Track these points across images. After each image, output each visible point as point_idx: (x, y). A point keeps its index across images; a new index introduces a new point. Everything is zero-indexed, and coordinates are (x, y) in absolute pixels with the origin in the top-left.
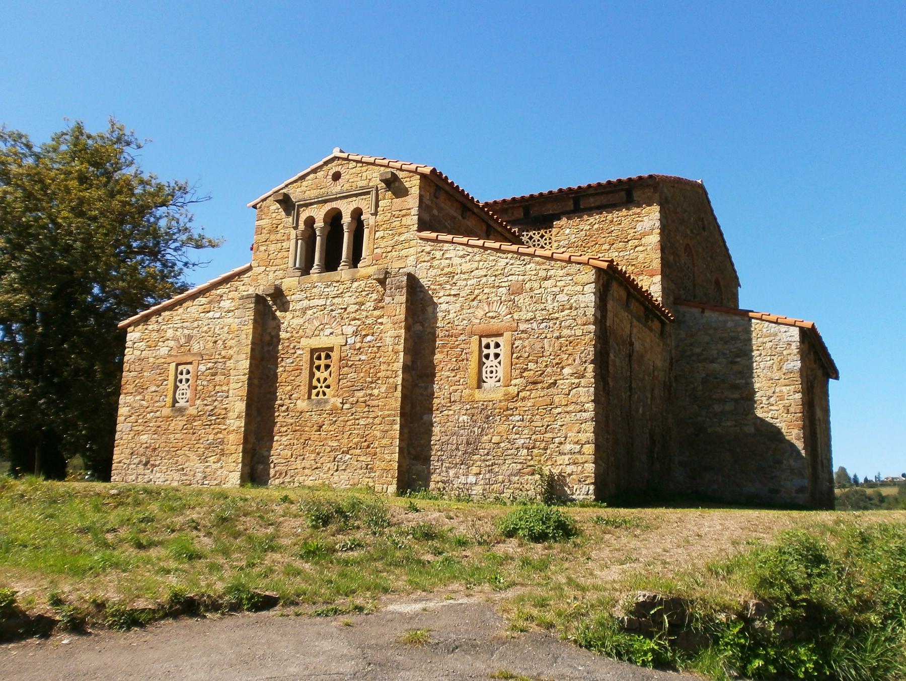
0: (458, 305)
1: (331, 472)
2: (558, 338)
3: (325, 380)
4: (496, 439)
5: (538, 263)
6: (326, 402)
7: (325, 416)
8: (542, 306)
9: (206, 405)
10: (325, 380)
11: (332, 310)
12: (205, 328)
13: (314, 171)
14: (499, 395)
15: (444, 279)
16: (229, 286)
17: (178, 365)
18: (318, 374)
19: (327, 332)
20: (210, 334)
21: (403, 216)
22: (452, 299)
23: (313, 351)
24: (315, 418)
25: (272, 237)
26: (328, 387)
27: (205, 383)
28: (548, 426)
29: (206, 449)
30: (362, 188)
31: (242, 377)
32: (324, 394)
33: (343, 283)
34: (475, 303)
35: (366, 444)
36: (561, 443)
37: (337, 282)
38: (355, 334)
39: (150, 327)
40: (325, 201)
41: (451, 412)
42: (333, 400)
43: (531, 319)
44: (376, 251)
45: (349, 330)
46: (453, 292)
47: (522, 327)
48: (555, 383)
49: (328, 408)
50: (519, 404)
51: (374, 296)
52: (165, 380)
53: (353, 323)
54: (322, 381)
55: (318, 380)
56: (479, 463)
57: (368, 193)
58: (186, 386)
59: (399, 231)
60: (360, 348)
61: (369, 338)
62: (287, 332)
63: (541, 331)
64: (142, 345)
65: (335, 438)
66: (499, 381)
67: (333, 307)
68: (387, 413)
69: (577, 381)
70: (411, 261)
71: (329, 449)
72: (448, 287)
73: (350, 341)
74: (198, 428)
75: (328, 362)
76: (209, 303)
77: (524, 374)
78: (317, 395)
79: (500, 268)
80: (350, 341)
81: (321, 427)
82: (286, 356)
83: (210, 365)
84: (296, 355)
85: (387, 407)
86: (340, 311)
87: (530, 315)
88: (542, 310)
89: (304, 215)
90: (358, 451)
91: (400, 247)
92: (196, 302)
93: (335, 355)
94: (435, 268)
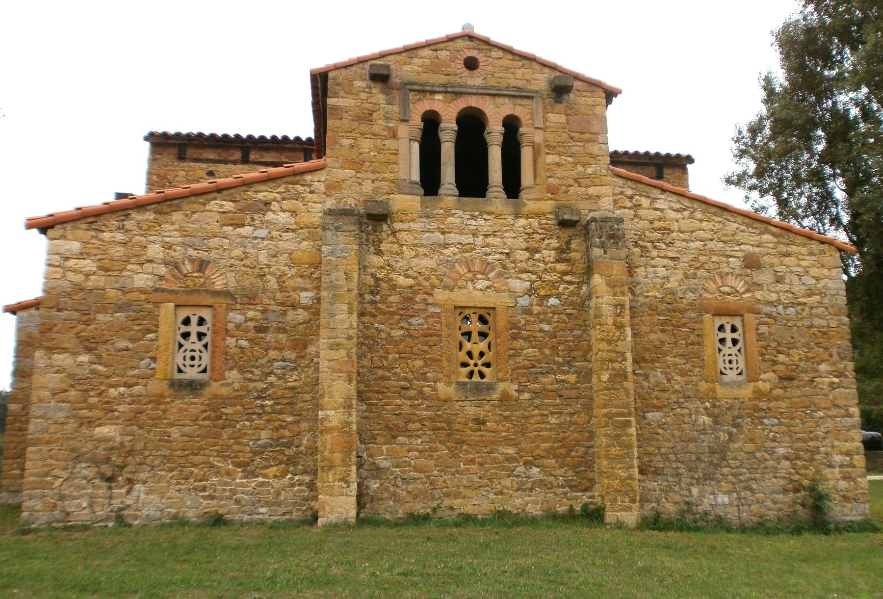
0: (681, 272)
2: (810, 327)
3: (482, 354)
4: (750, 447)
5: (773, 234)
6: (490, 388)
7: (487, 407)
8: (787, 287)
9: (251, 380)
10: (482, 354)
11: (486, 255)
12: (237, 252)
14: (746, 392)
15: (657, 235)
16: (282, 189)
17: (177, 306)
19: (482, 284)
20: (247, 262)
21: (588, 141)
22: (672, 263)
25: (364, 128)
26: (488, 365)
27: (244, 343)
28: (811, 432)
29: (255, 453)
30: (518, 89)
32: (482, 375)
33: (498, 216)
34: (701, 272)
36: (827, 454)
38: (529, 292)
39: (106, 236)
40: (459, 94)
41: (686, 411)
42: (501, 386)
43: (776, 301)
45: (518, 285)
46: (671, 254)
47: (768, 309)
48: (812, 381)
50: (772, 404)
51: (554, 243)
52: (151, 332)
53: (524, 276)
56: (730, 478)
57: (531, 98)
58: (199, 346)
60: (539, 313)
61: (553, 301)
62: (407, 276)
63: (787, 317)
64: (89, 265)
65: (508, 441)
66: (740, 374)
67: (488, 250)
68: (614, 410)
69: (836, 380)
70: (606, 203)
72: (663, 246)
73: (524, 301)
74: (236, 418)
76: (241, 210)
77: (775, 368)
78: (471, 374)
79: (730, 233)
81: (484, 423)
82: (411, 312)
83: (251, 314)
86: (498, 256)
87: (774, 297)
88: (787, 292)
91: (587, 182)
92: (213, 205)
93: (501, 321)
94: (641, 219)
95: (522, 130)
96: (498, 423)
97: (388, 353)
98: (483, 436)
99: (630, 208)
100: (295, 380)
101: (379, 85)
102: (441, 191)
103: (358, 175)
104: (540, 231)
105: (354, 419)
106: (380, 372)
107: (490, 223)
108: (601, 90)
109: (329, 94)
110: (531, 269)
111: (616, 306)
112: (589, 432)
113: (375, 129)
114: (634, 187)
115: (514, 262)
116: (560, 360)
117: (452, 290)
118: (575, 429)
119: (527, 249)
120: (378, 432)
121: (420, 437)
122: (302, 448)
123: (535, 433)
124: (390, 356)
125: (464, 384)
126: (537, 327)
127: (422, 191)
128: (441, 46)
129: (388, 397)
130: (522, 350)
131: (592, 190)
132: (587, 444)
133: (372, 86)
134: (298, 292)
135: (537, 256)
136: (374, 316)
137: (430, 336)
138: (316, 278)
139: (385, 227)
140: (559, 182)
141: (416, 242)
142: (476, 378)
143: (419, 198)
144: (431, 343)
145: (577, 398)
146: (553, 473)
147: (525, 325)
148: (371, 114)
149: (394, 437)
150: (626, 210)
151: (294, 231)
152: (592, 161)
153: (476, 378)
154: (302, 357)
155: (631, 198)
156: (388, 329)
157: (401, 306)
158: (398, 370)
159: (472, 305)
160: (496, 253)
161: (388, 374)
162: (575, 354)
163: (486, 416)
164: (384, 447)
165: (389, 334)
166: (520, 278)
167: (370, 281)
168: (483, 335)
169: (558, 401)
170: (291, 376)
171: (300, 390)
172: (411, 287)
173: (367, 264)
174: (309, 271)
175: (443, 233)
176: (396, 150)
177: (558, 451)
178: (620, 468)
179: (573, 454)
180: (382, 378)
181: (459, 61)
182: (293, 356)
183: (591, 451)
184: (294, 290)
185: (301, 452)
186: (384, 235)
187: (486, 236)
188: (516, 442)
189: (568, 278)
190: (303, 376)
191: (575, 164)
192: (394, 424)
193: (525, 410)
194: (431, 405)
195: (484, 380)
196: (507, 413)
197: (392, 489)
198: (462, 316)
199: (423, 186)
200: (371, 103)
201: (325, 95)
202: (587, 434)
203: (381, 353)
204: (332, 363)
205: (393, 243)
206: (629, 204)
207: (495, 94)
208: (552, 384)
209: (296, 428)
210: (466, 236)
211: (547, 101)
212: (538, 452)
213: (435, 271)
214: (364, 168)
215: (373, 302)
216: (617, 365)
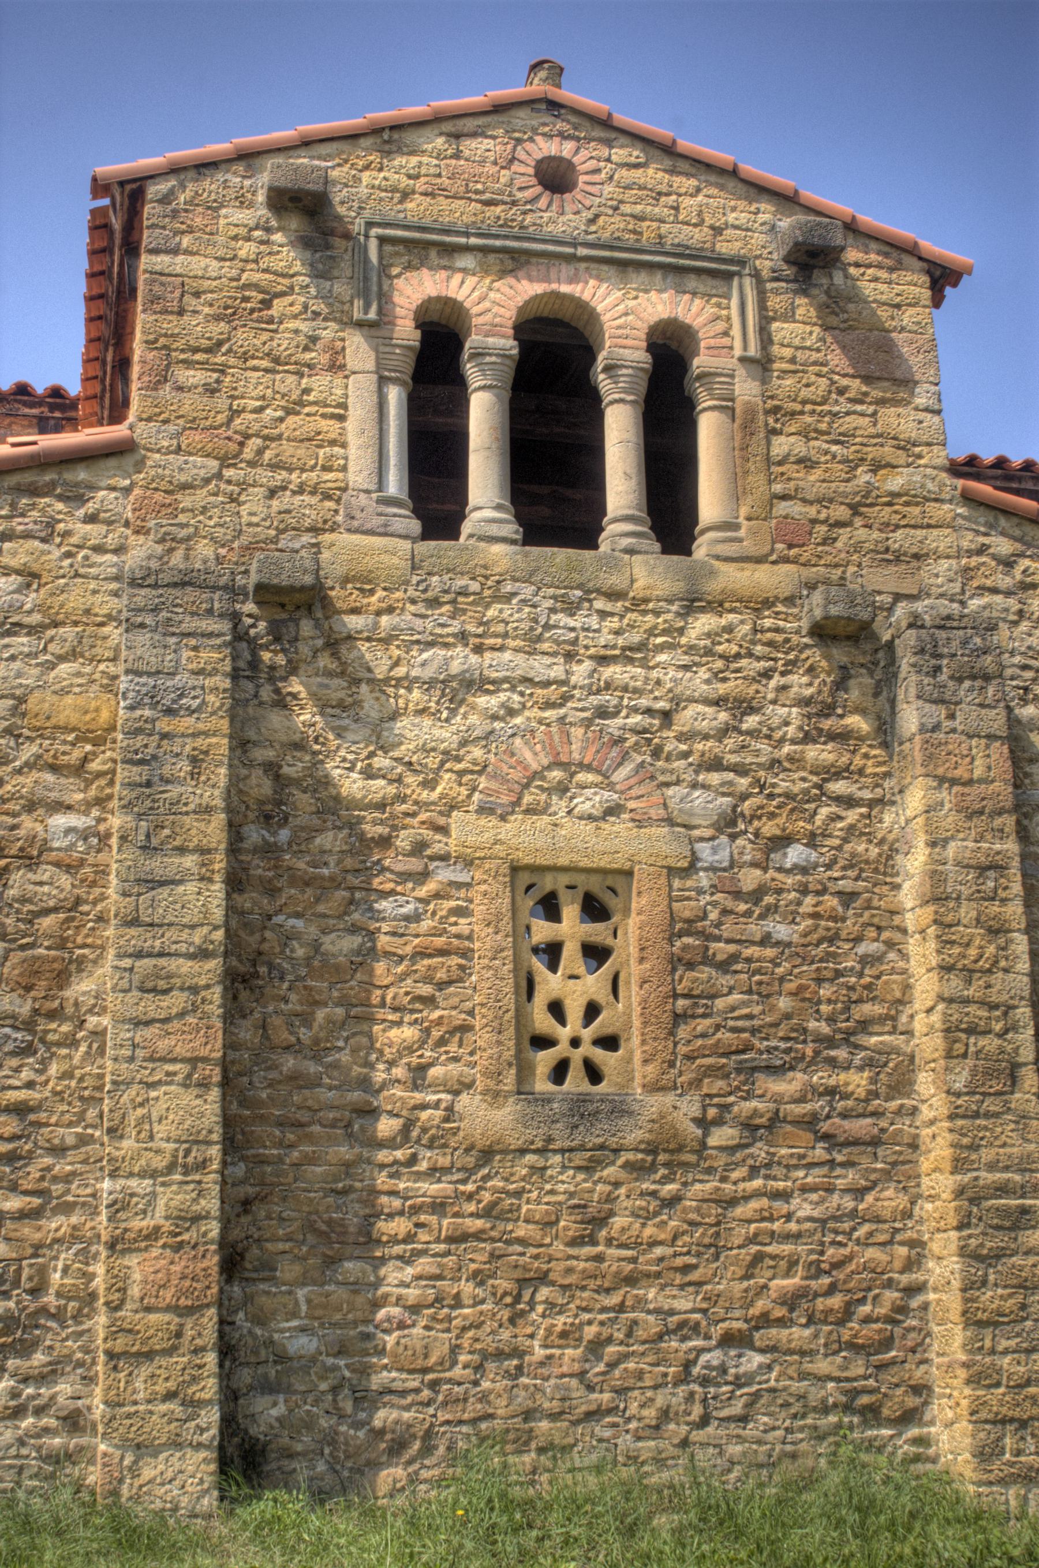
1: (676, 1430)
10: (592, 1011)
11: (602, 713)
13: (454, 124)
18: (551, 984)
19: (590, 801)
21: (881, 402)
23: (521, 874)
24: (565, 1181)
25: (244, 338)
26: (609, 1042)
31: (185, 966)
32: (594, 1074)
33: (639, 604)
35: (836, 1301)
37: (613, 595)
44: (782, 508)
49: (634, 1136)
53: (715, 778)
54: (574, 1011)
55: (556, 1009)
59: (872, 453)
61: (795, 854)
62: (369, 774)
67: (609, 699)
68: (988, 1177)
71: (652, 1324)
75: (598, 932)
78: (560, 1072)
80: (704, 850)
81: (601, 1221)
84: (423, 892)
85: (987, 1155)
86: (636, 719)
89: (415, 289)
90: (798, 1334)
95: (700, 363)
96: (646, 1216)
97: (317, 1003)
98: (599, 1258)
99: (1008, 593)
100: (30, 1085)
101: (294, 223)
102: (467, 528)
103: (228, 473)
104: (759, 649)
105: (212, 1204)
106: (289, 1063)
107: (614, 623)
108: (918, 264)
109: (147, 238)
110: (734, 759)
111: (982, 870)
112: (912, 1244)
113: (283, 343)
114: (1017, 533)
115: (681, 738)
116: (825, 1029)
117: (503, 818)
118: (871, 1234)
119: (717, 702)
120: (281, 1246)
121: (408, 1262)
122: (50, 1299)
123: (754, 1249)
124: (321, 1014)
125: (547, 1100)
126: (755, 930)
127: (415, 526)
128: (470, 124)
129: (310, 1138)
130: (713, 997)
131: (899, 539)
132: (905, 1279)
133: (274, 223)
134: (41, 811)
135: (751, 722)
136: (272, 892)
137: (443, 952)
138: (100, 775)
139: (306, 627)
140: (812, 511)
141: (401, 671)
142: (575, 1082)
143: (407, 545)
144: (441, 975)
145: (875, 1142)
146: (808, 1367)
147: (718, 925)
148: (267, 304)
149: (332, 1262)
150: (998, 599)
151: (33, 630)
152: (902, 458)
153: (575, 1082)
154: (52, 1015)
155: (1008, 563)
156: (313, 931)
157: (349, 863)
158: (345, 1057)
159: (563, 861)
160: (635, 710)
161: (313, 1068)
162: (868, 1009)
163: (610, 1199)
164: (301, 1293)
165: (316, 946)
166: (705, 787)
167: (261, 786)
168: (596, 954)
169: (819, 1152)
170: (17, 1070)
171: (43, 1116)
172: (381, 806)
173: (252, 734)
174: (77, 754)
175: (478, 650)
176: (339, 405)
177: (820, 1303)
178: (1006, 1352)
179: (866, 1309)
180: (297, 1080)
181: (522, 169)
182: (25, 1009)
183: (915, 1303)
184: (31, 807)
185: (44, 1311)
186: (304, 650)
187: (603, 660)
188: (695, 1276)
189: (838, 787)
190: (54, 1069)
191: (852, 465)
192: (329, 1222)
193: (724, 1179)
194: (444, 1161)
195: (602, 1088)
196: (671, 1188)
197: (324, 1423)
198: (537, 894)
199: (418, 512)
200: (266, 271)
201: (132, 249)
202: (903, 1251)
203: (295, 1003)
204: (149, 1032)
205: (329, 674)
206: (1005, 582)
207: (623, 262)
208: (801, 1100)
209: (26, 1230)
210: (548, 660)
211: (769, 286)
212: (761, 1305)
213: (458, 759)
214: (248, 453)
215: (268, 850)
216: (989, 1043)
